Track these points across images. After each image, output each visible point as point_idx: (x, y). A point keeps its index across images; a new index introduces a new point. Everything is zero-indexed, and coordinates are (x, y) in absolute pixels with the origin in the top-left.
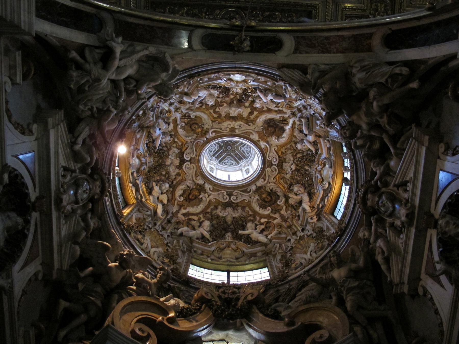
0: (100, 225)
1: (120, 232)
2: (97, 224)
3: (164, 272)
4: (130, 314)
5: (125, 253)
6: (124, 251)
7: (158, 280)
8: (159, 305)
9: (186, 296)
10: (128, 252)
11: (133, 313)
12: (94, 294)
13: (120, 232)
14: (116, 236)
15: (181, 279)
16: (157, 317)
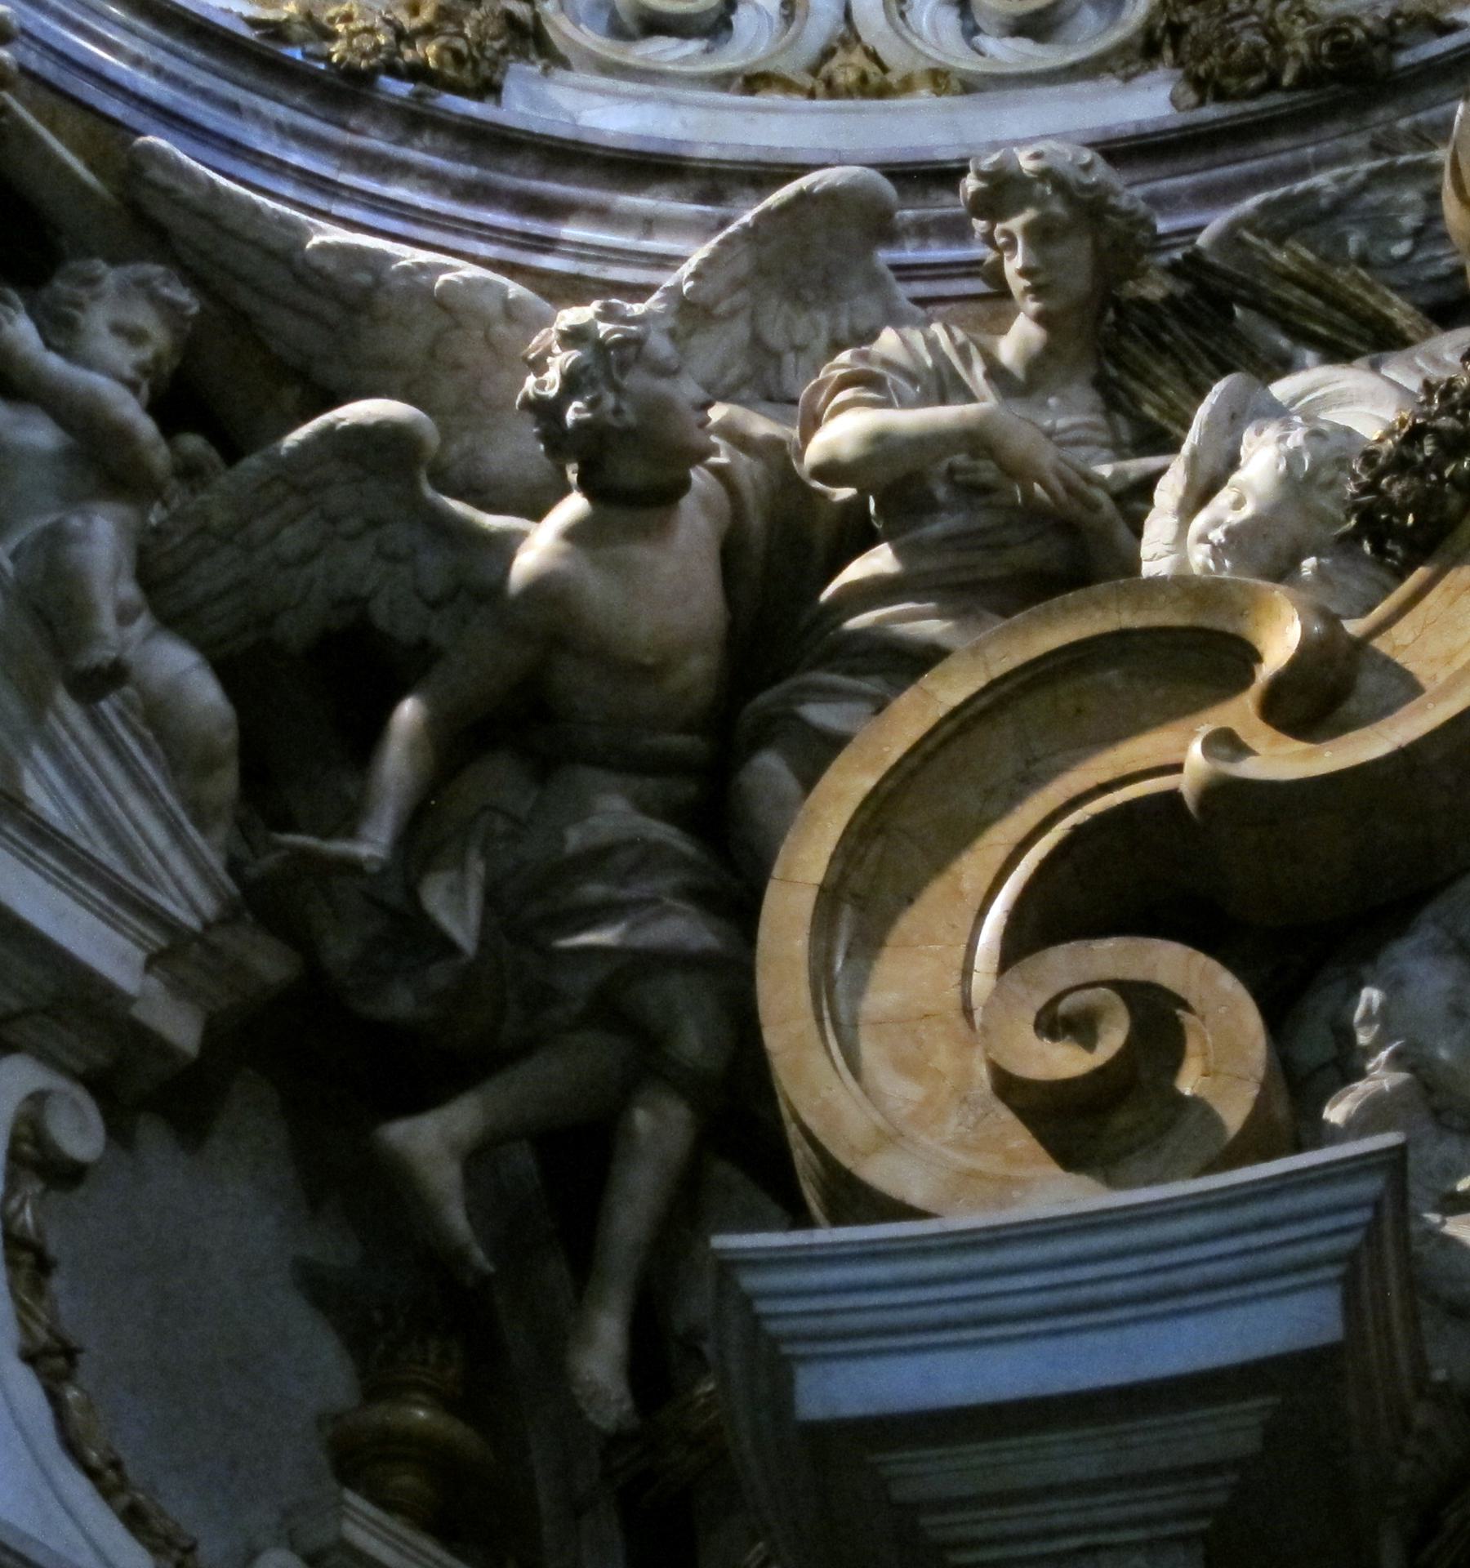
0: (182, 295)
1: (413, 155)
2: (144, 317)
3: (1029, 214)
4: (909, 922)
5: (553, 377)
6: (538, 366)
7: (1040, 318)
8: (1123, 635)
9: (1409, 221)
10: (574, 355)
11: (936, 892)
12: (594, 891)
13: (413, 155)
14: (387, 258)
15: (1273, 84)
16: (1170, 759)
